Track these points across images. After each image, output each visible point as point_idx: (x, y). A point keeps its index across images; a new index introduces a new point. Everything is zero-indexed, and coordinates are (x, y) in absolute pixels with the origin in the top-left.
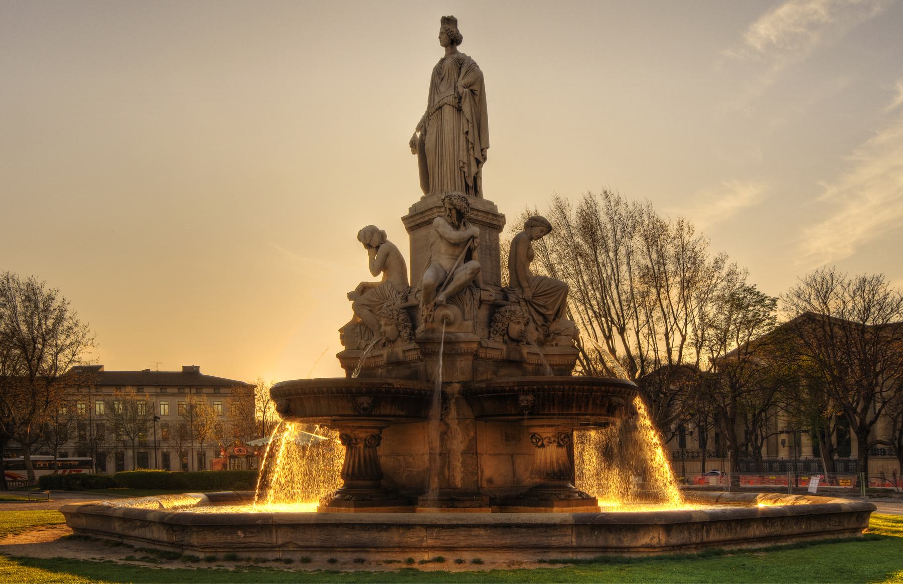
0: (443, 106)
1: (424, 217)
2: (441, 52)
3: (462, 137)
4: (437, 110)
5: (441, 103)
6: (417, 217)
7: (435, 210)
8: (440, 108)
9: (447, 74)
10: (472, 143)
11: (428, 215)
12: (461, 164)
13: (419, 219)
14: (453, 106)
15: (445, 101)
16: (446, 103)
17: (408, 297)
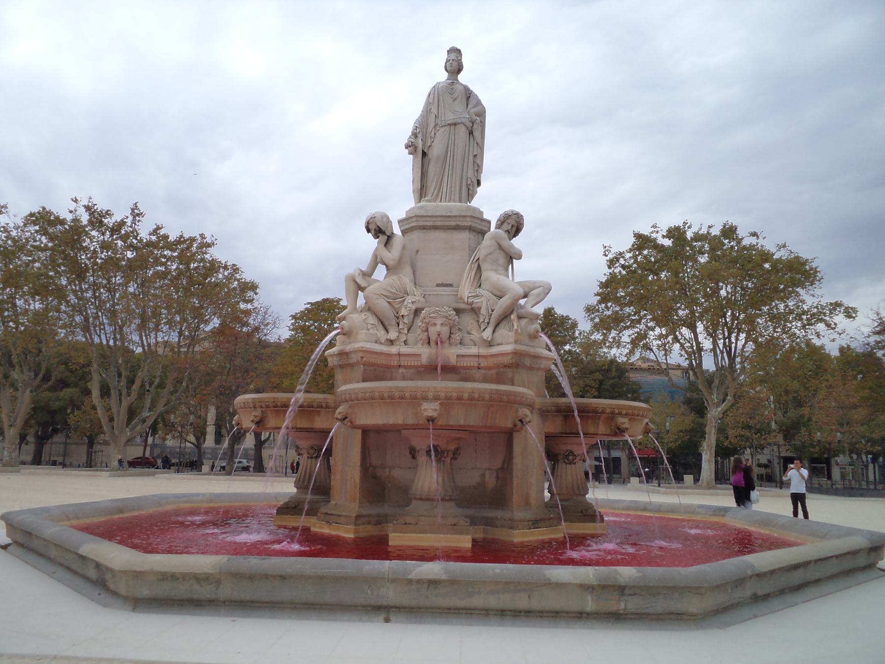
0: (459, 124)
1: (449, 221)
2: (443, 76)
3: (471, 157)
4: (450, 125)
5: (459, 121)
6: (439, 219)
7: (468, 219)
8: (455, 124)
9: (460, 97)
10: (478, 166)
11: (456, 221)
12: (469, 182)
13: (440, 221)
14: (467, 128)
15: (463, 120)
16: (462, 123)
17: (426, 296)
